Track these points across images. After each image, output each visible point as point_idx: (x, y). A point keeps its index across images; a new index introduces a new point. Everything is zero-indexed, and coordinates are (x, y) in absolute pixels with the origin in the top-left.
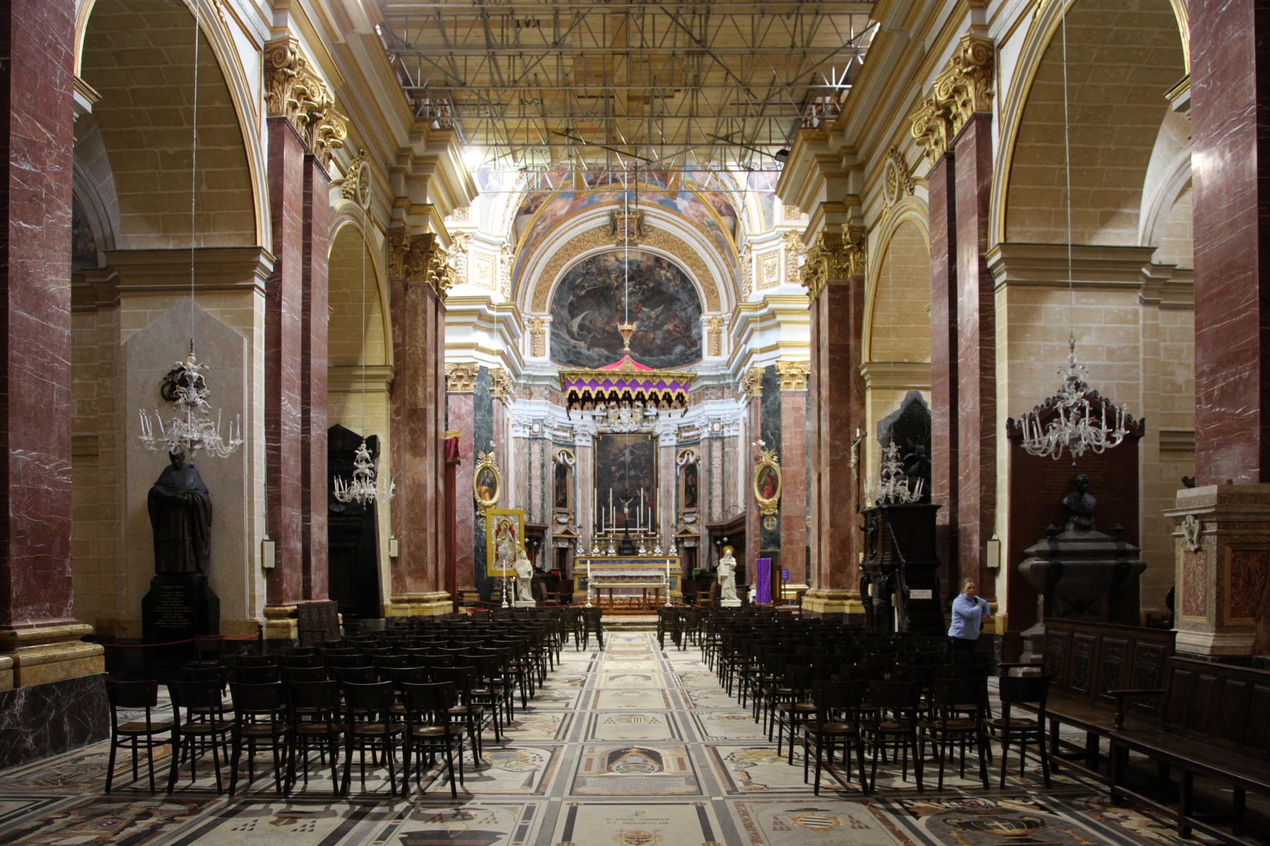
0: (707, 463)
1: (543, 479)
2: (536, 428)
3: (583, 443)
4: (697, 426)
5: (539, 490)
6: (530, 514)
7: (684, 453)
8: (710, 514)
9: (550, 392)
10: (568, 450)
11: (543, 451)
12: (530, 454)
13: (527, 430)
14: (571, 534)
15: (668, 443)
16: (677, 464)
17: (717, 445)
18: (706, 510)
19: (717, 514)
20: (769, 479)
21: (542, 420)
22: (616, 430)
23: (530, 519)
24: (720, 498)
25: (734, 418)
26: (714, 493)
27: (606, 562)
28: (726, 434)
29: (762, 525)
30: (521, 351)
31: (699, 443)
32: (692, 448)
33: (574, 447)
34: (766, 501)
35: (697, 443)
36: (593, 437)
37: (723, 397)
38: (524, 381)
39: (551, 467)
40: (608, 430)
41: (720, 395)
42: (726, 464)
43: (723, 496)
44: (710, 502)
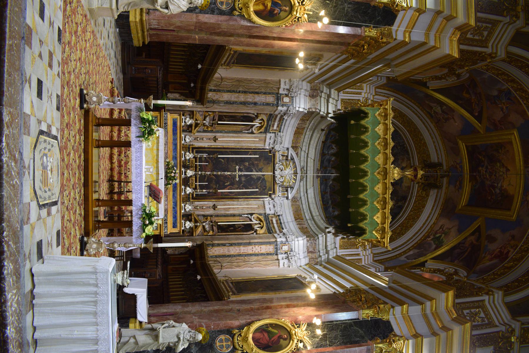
0: (256, 241)
1: (244, 103)
2: (286, 100)
3: (268, 141)
4: (285, 231)
5: (236, 100)
6: (214, 91)
7: (260, 220)
8: (213, 245)
9: (313, 113)
10: (264, 126)
11: (268, 104)
12: (265, 93)
13: (286, 92)
14: (195, 128)
15: (267, 206)
16: (252, 214)
17: (270, 249)
18: (216, 242)
19: (214, 251)
20: (275, 338)
21: (292, 104)
22: (277, 165)
23: (211, 90)
24: (227, 253)
25: (294, 263)
26: (231, 248)
27: (175, 149)
28: (280, 257)
29: (221, 332)
30: (347, 90)
31: (271, 233)
32: (265, 227)
33: (266, 131)
34: (250, 336)
35: (270, 231)
36: (273, 148)
37: (309, 252)
38: (325, 91)
39: (251, 111)
40: (277, 160)
41: (311, 250)
42: (255, 258)
43: (229, 256)
44: (224, 245)
